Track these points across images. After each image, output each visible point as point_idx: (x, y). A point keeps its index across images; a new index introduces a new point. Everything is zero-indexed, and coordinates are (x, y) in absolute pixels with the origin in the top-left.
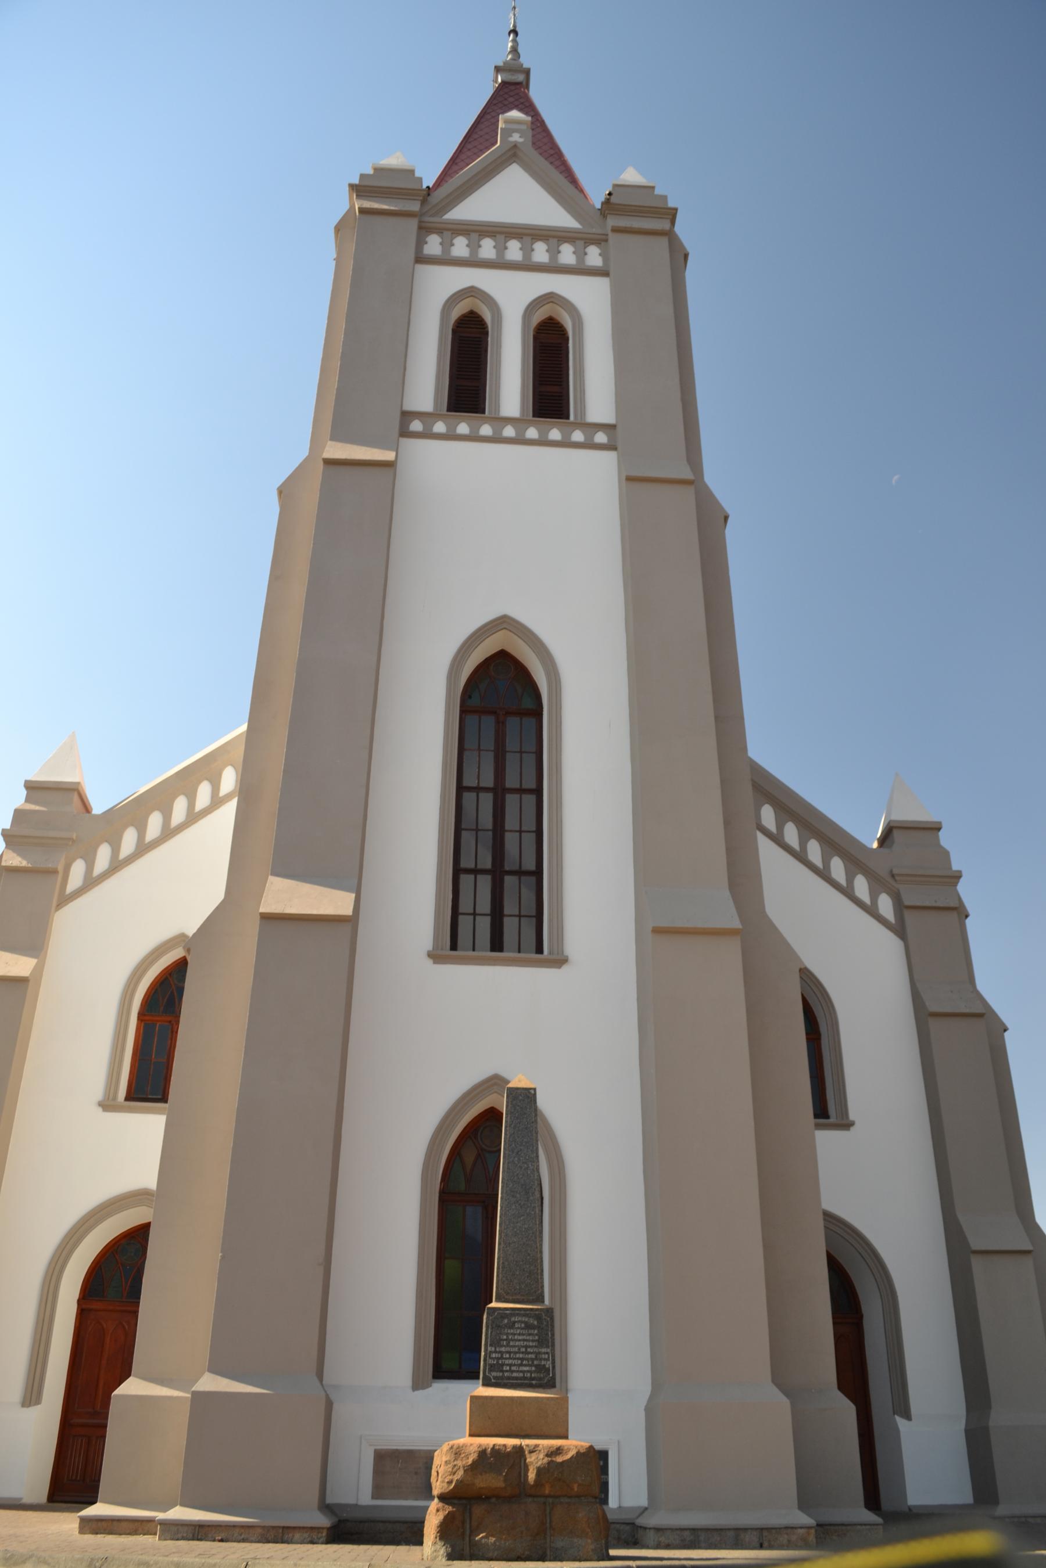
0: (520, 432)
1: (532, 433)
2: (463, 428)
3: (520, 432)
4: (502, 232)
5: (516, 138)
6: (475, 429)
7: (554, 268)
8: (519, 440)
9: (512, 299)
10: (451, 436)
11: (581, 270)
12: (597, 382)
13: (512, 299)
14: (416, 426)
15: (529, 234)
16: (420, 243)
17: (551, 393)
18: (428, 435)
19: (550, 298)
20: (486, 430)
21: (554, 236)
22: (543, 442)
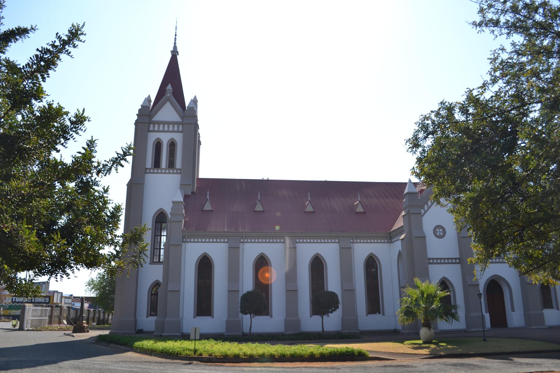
0: (165, 171)
1: (167, 171)
2: (156, 171)
3: (165, 171)
4: (164, 123)
5: (169, 95)
6: (158, 171)
7: (173, 131)
8: (165, 173)
9: (165, 138)
10: (154, 173)
11: (178, 132)
12: (178, 164)
13: (165, 138)
14: (148, 171)
15: (169, 123)
16: (149, 127)
17: (171, 164)
18: (150, 173)
19: (172, 139)
20: (160, 171)
21: (174, 123)
22: (169, 173)
